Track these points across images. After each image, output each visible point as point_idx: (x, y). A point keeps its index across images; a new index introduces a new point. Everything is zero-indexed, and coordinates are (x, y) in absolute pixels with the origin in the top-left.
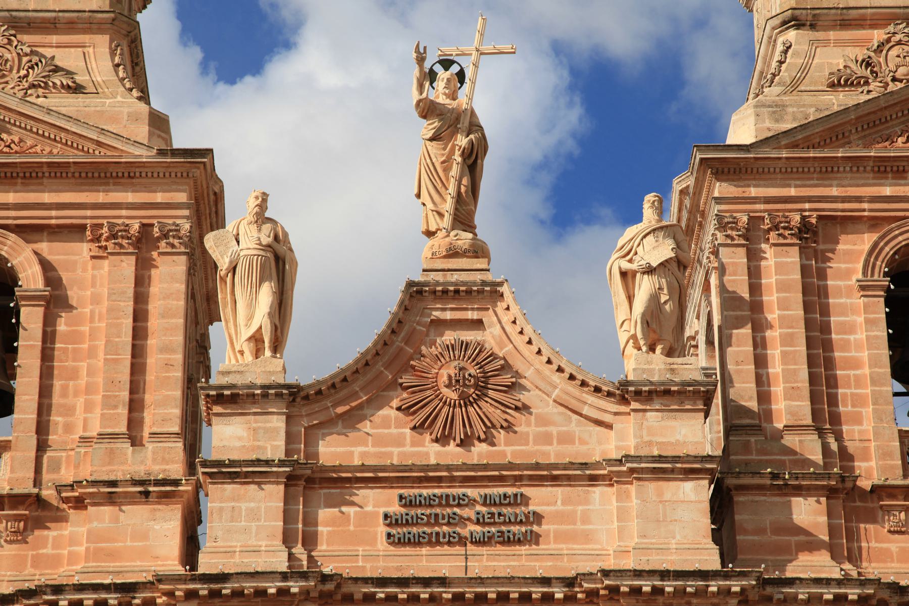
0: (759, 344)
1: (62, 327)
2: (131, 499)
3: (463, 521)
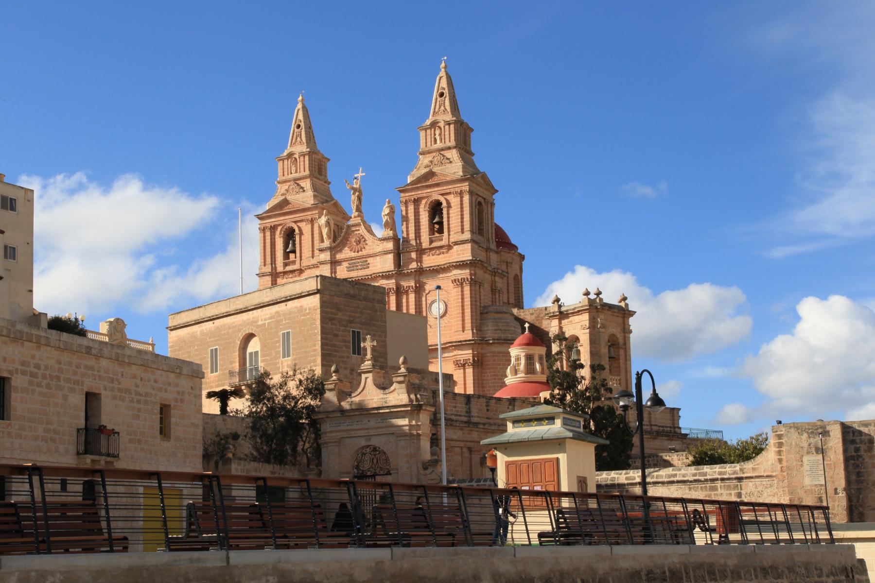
0: (407, 224)
1: (302, 238)
2: (312, 268)
3: (357, 266)
